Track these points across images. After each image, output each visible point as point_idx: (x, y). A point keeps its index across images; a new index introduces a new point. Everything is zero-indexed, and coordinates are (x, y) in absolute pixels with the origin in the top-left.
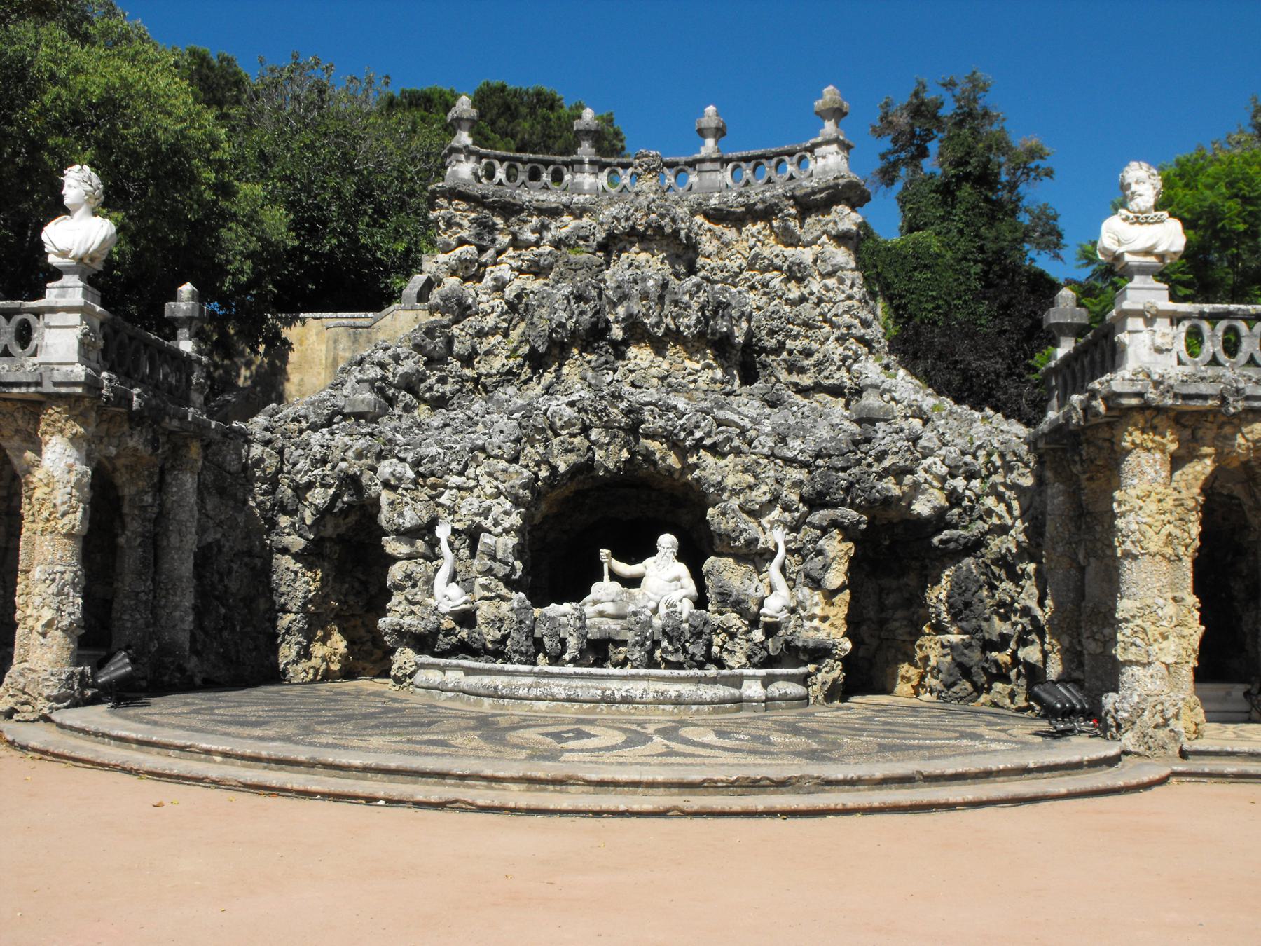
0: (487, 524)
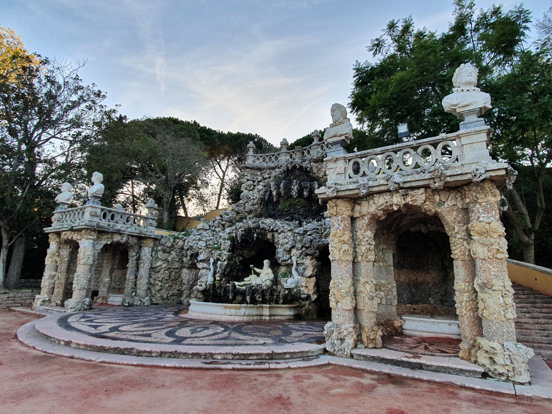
0: (220, 258)
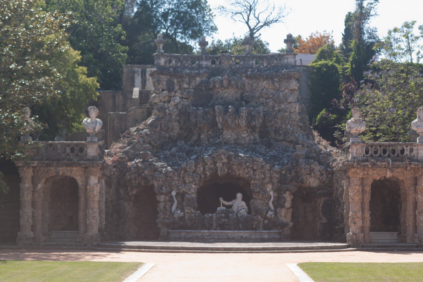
0: (187, 191)
